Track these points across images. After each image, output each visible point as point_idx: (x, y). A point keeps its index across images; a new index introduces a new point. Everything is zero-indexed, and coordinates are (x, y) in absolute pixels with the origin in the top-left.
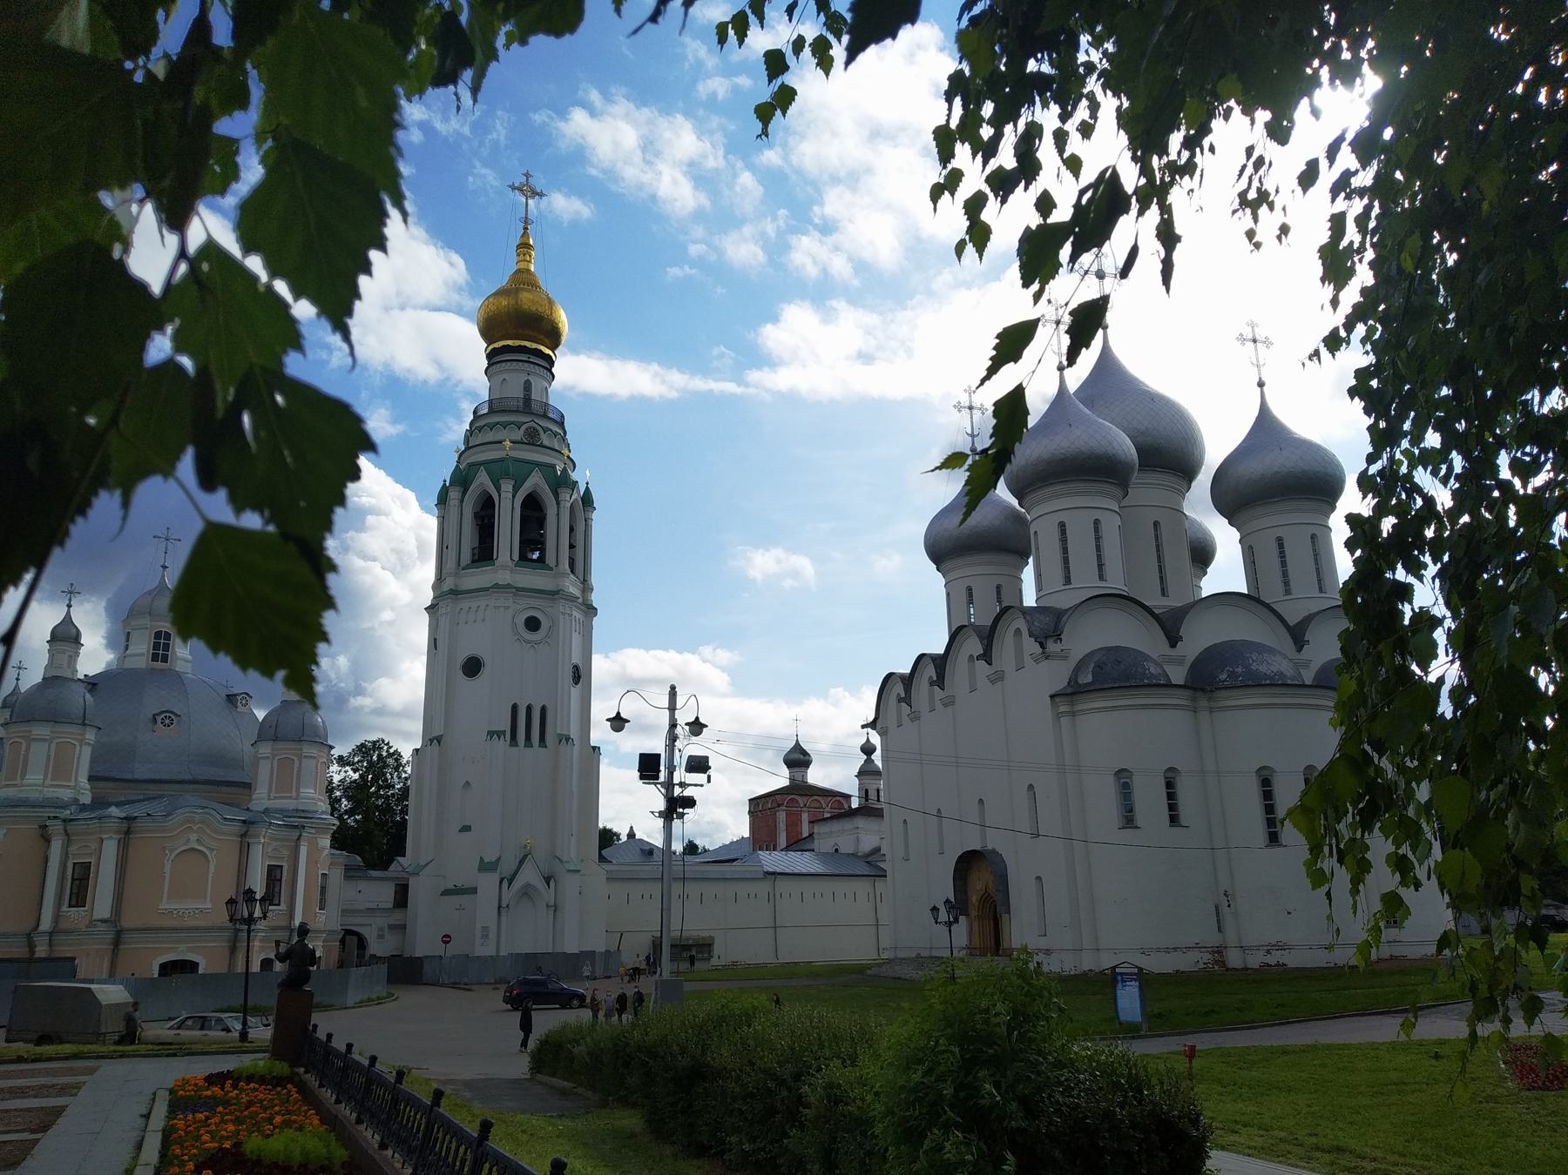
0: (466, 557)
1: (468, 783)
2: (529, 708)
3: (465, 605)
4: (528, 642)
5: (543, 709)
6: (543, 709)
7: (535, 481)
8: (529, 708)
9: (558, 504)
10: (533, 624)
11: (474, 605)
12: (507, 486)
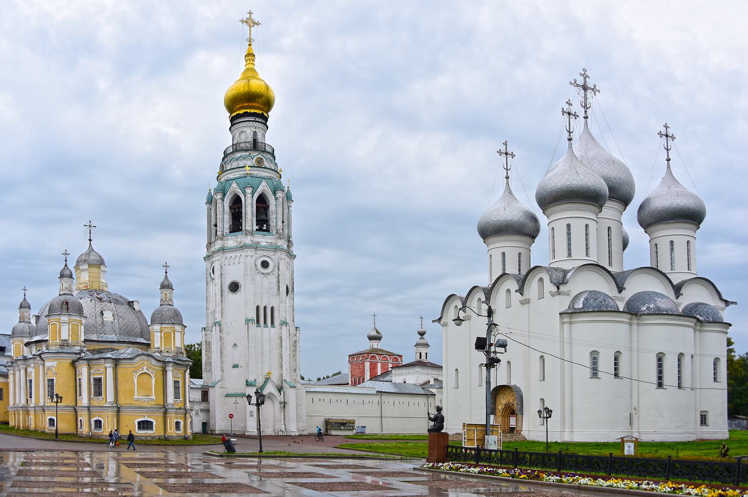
0: (227, 231)
1: (235, 345)
2: (265, 308)
3: (228, 255)
4: (264, 274)
5: (272, 308)
6: (272, 308)
7: (264, 187)
8: (265, 308)
9: (276, 199)
10: (265, 264)
11: (233, 255)
12: (249, 191)
